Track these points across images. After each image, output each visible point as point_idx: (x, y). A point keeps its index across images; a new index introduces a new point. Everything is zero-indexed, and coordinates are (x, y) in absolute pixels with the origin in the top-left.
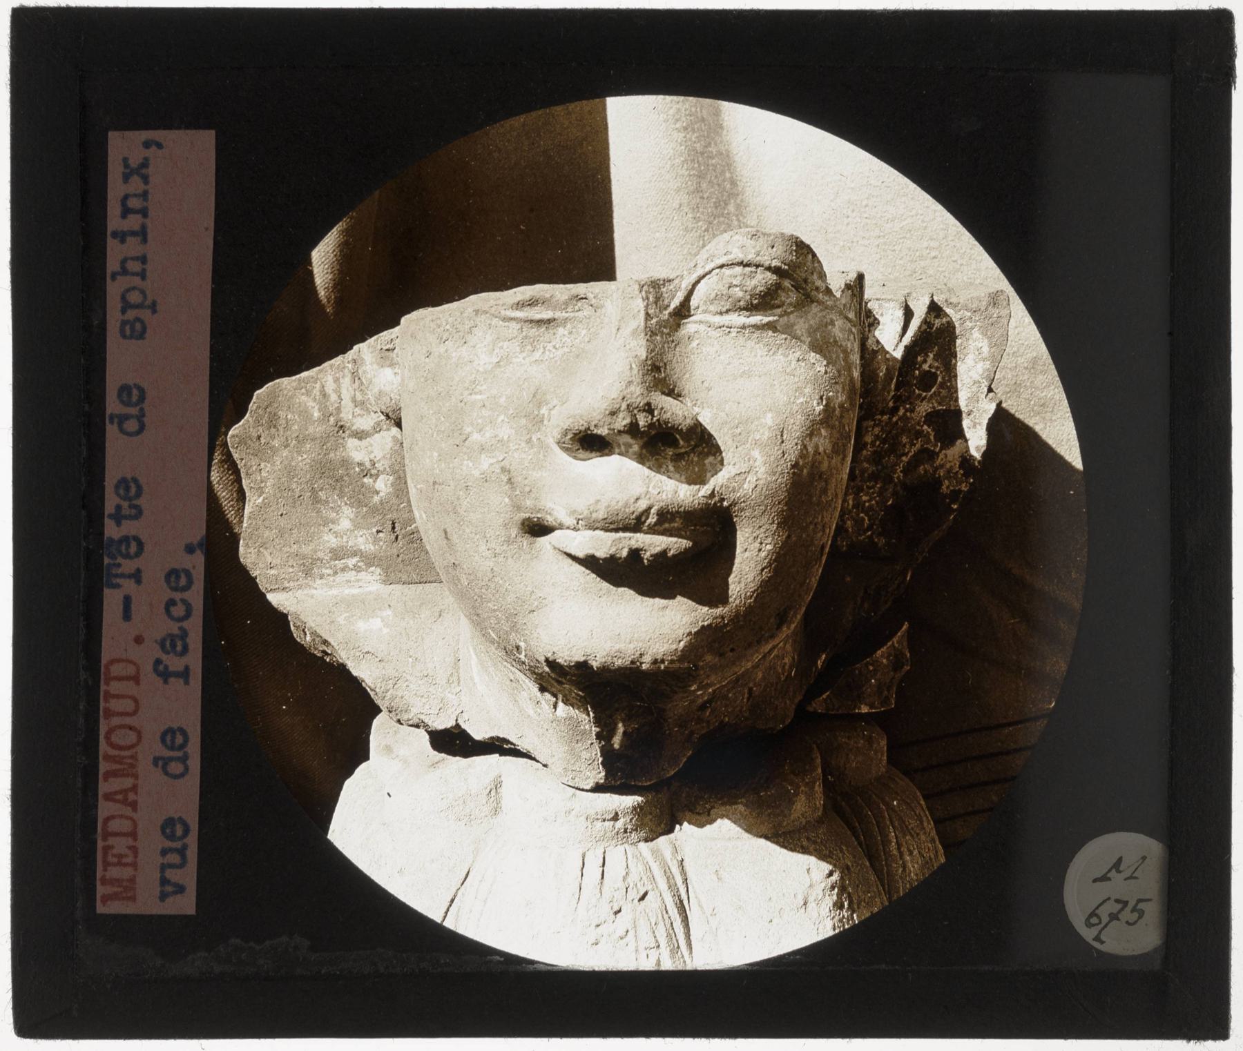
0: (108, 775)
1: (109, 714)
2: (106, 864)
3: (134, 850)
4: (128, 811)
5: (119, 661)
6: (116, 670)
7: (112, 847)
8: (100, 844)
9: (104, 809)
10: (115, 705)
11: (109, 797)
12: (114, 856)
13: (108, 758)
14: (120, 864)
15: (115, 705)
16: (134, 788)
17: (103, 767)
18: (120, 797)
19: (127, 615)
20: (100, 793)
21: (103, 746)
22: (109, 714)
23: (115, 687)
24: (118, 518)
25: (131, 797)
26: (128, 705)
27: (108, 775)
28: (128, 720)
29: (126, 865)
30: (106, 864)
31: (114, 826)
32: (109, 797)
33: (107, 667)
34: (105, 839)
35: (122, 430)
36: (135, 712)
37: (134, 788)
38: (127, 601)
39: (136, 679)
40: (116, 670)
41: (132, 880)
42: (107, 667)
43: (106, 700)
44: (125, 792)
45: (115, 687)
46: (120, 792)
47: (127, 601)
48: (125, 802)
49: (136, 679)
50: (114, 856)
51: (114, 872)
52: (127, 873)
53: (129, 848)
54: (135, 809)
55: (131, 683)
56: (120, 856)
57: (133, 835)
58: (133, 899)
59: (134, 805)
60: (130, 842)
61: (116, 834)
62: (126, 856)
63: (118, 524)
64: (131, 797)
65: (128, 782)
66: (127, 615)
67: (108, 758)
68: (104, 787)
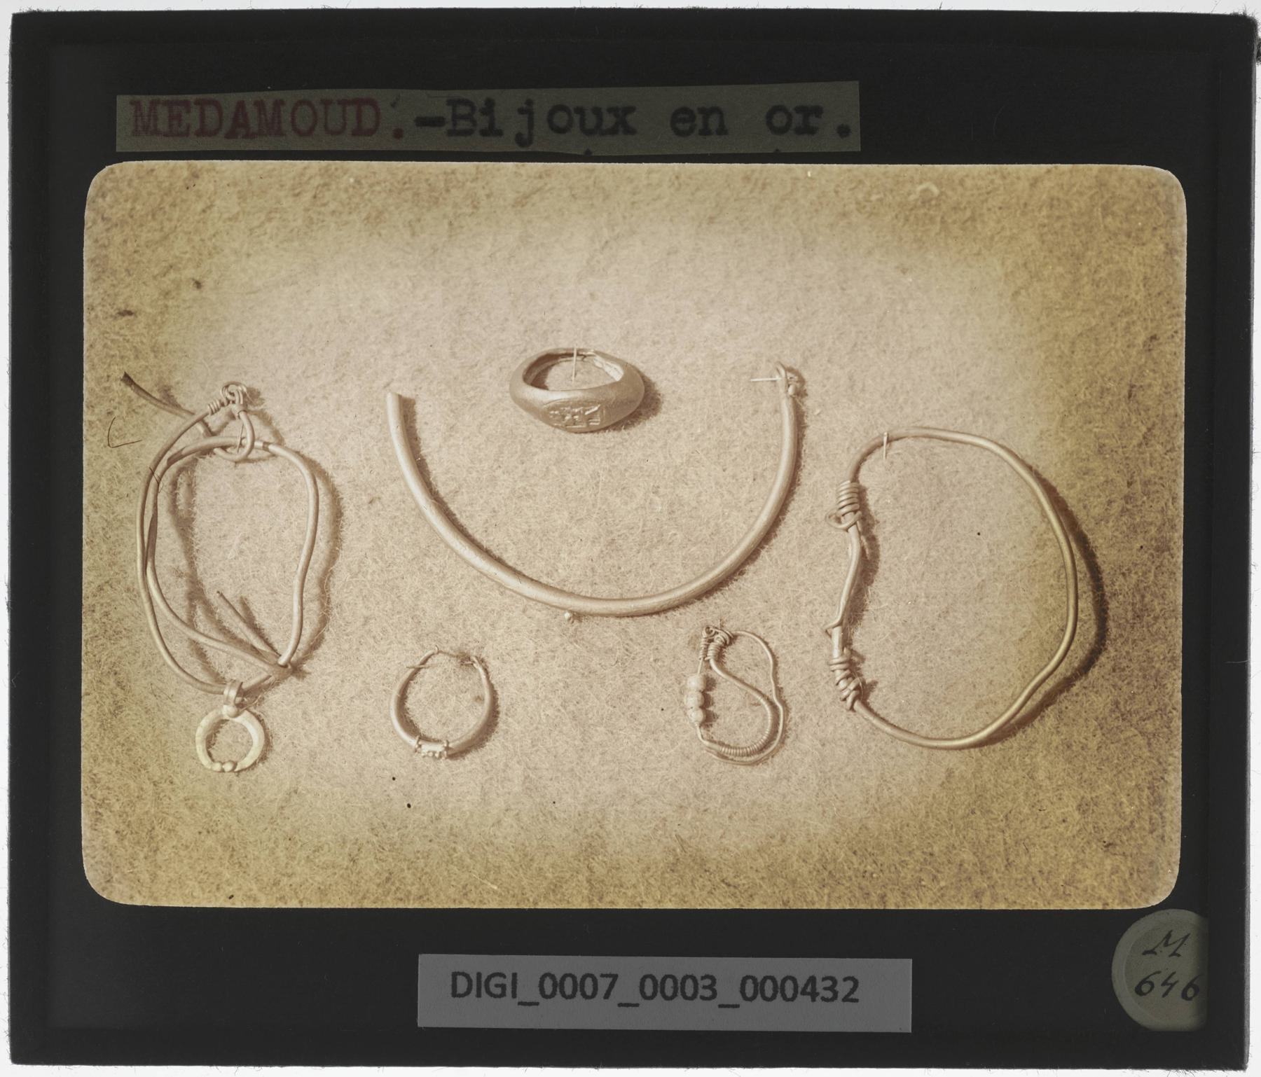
0: (260, 105)
2: (169, 104)
3: (187, 134)
4: (227, 124)
5: (378, 114)
6: (368, 111)
7: (188, 112)
8: (192, 98)
9: (230, 100)
11: (241, 105)
13: (278, 104)
14: (171, 118)
17: (269, 97)
19: (423, 122)
23: (351, 111)
27: (260, 105)
29: (171, 126)
30: (169, 104)
31: (211, 112)
32: (241, 105)
34: (197, 103)
38: (437, 122)
40: (368, 111)
41: (156, 132)
42: (372, 103)
46: (245, 115)
47: (437, 122)
51: (163, 113)
52: (163, 126)
53: (189, 127)
56: (179, 117)
58: (136, 133)
60: (196, 125)
62: (180, 125)
66: (423, 122)
67: (278, 104)
68: (250, 98)
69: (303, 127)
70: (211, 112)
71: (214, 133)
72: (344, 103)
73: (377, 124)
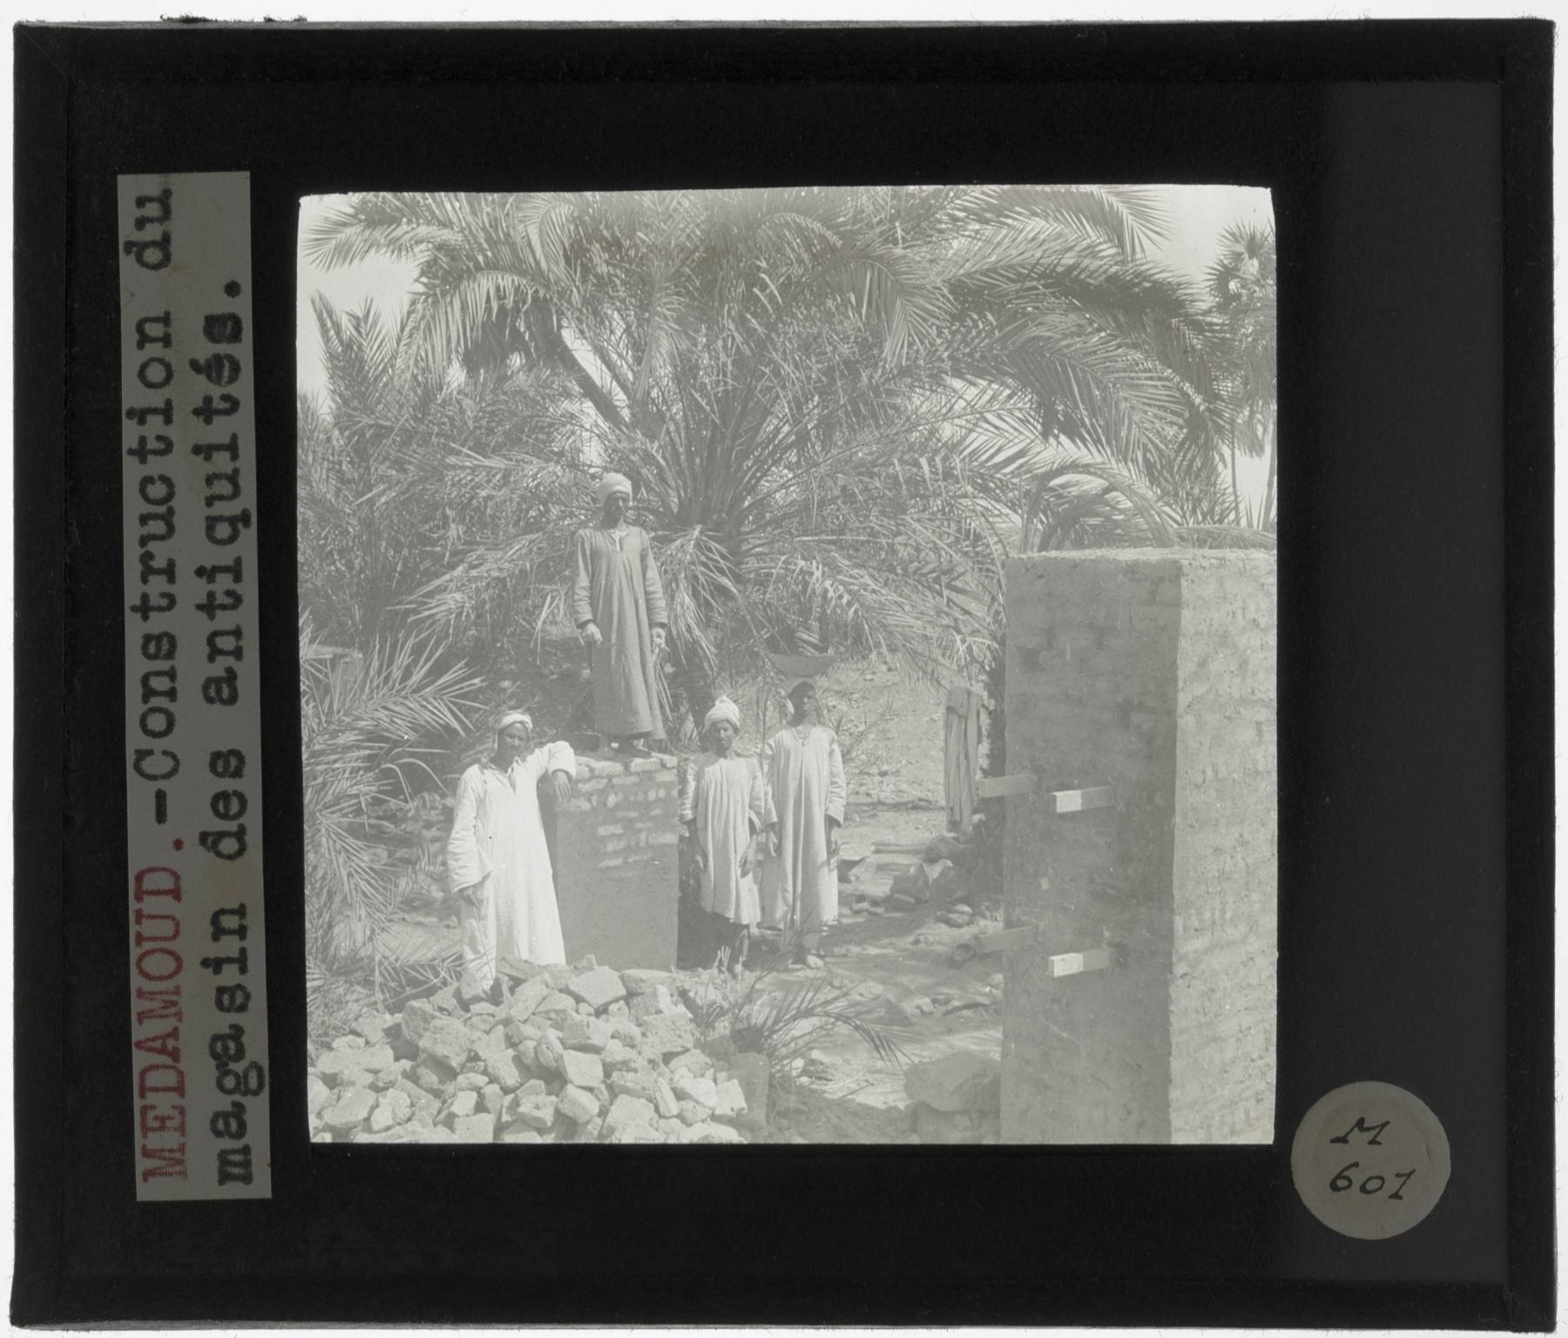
0: (142, 1016)
1: (140, 939)
4: (167, 1060)
5: (151, 870)
6: (149, 882)
9: (140, 1059)
10: (149, 928)
12: (156, 1118)
13: (141, 994)
14: (162, 1128)
15: (149, 928)
16: (174, 1034)
17: (136, 1005)
18: (158, 1044)
20: (135, 1037)
21: (136, 981)
22: (140, 939)
23: (150, 905)
24: (145, 609)
25: (171, 1043)
26: (166, 928)
28: (164, 945)
31: (153, 1079)
33: (140, 878)
35: (140, 260)
36: (175, 937)
37: (174, 1034)
38: (161, 797)
39: (176, 894)
42: (140, 878)
43: (138, 922)
46: (155, 1039)
47: (161, 797)
48: (163, 1051)
50: (156, 1118)
54: (175, 1055)
55: (169, 898)
57: (180, 1089)
61: (156, 1089)
63: (143, 461)
64: (171, 1043)
65: (166, 1025)
67: (141, 994)
68: (138, 1032)
69: (171, 964)
70: (153, 1079)
71: (181, 1074)
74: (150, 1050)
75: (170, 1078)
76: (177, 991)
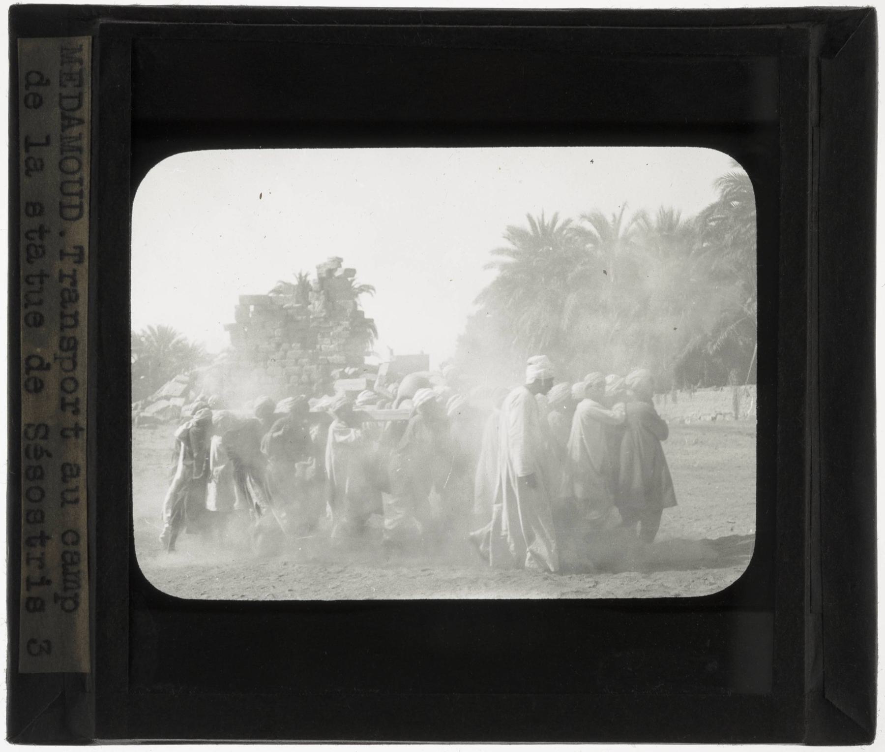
0: (80, 137)
4: (67, 114)
11: (81, 121)
12: (74, 80)
15: (76, 188)
18: (73, 122)
23: (76, 200)
32: (81, 121)
40: (75, 212)
44: (70, 126)
45: (76, 200)
49: (62, 206)
50: (74, 80)
59: (64, 117)
64: (66, 122)
65: (67, 133)
72: (80, 194)
73: (66, 219)
74: (77, 119)
75: (67, 103)
76: (62, 152)
